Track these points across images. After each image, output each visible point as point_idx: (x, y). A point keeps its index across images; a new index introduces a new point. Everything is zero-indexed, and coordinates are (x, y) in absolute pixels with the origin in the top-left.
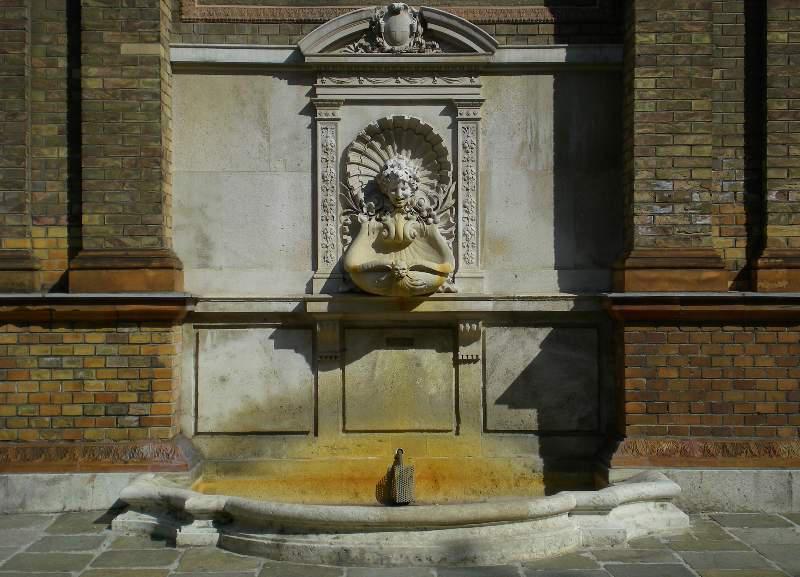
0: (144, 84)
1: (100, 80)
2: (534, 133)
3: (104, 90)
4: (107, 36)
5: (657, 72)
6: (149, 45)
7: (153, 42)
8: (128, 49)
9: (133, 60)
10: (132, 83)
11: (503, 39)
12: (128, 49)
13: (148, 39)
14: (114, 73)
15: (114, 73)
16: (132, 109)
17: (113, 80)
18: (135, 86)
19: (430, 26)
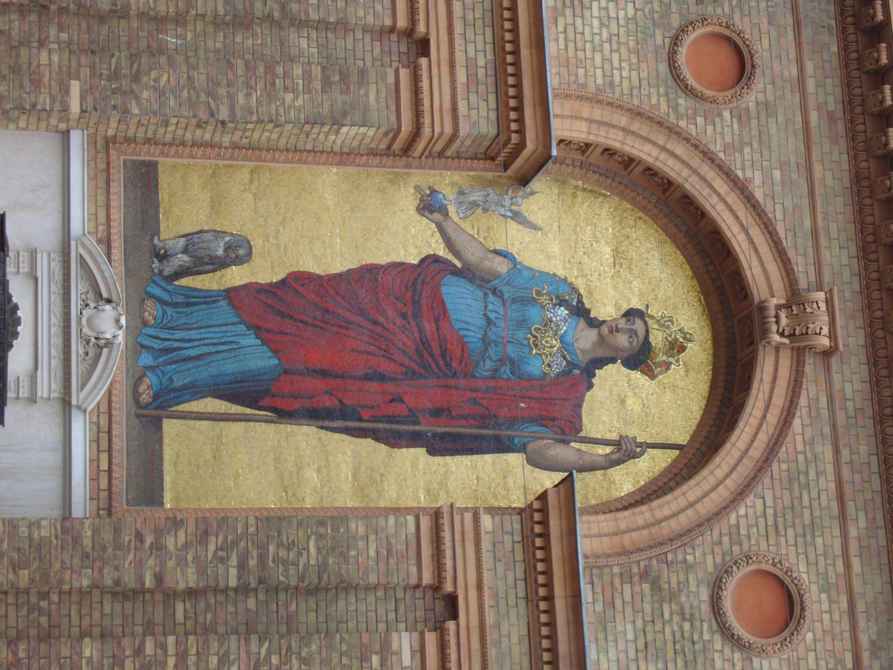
0: (44, 100)
1: (47, 62)
2: (6, 448)
3: (38, 65)
4: (85, 72)
5: (57, 538)
6: (79, 104)
7: (81, 105)
8: (75, 88)
9: (67, 92)
10: (45, 88)
11: (95, 419)
12: (75, 88)
13: (84, 103)
14: (54, 75)
15: (54, 75)
16: (21, 87)
17: (47, 73)
18: (43, 90)
19: (105, 350)
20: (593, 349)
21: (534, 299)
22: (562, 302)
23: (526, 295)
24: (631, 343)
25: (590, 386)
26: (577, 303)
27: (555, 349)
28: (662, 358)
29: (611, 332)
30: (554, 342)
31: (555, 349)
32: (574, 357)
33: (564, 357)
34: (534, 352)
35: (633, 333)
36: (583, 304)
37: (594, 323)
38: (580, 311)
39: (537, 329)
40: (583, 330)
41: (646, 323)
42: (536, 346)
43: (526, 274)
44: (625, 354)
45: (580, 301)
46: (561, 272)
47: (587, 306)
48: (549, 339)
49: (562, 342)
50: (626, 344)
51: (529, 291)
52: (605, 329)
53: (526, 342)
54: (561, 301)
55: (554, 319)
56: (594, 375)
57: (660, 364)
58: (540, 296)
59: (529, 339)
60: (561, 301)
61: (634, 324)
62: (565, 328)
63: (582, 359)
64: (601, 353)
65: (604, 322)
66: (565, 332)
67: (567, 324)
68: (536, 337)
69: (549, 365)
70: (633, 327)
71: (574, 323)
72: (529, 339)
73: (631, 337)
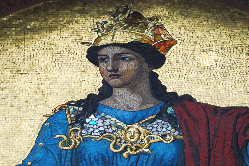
20: (140, 93)
21: (74, 148)
22: (80, 120)
23: (69, 156)
24: (131, 59)
25: (188, 98)
26: (80, 106)
27: (140, 129)
28: (148, 33)
29: (118, 76)
30: (132, 130)
31: (140, 129)
32: (151, 112)
33: (154, 120)
34: (147, 150)
35: (117, 58)
36: (81, 101)
37: (106, 91)
38: (91, 105)
39: (115, 146)
40: (116, 101)
41: (103, 46)
42: (138, 148)
43: (39, 155)
44: (145, 65)
45: (79, 103)
46: (38, 122)
47: (84, 97)
48: (128, 135)
49: (132, 122)
50: (133, 63)
51: (64, 152)
52: (113, 82)
53: (133, 159)
54: (77, 122)
55: (102, 129)
56: (174, 94)
57: (156, 35)
58: (70, 143)
59: (129, 155)
60: (77, 122)
61: (107, 56)
62: (114, 119)
63: (152, 103)
64: (145, 86)
65: (104, 82)
66: (118, 118)
67: (108, 116)
68: (126, 148)
69: (164, 136)
70: (111, 57)
71: (106, 110)
72: (129, 155)
73: (123, 59)
